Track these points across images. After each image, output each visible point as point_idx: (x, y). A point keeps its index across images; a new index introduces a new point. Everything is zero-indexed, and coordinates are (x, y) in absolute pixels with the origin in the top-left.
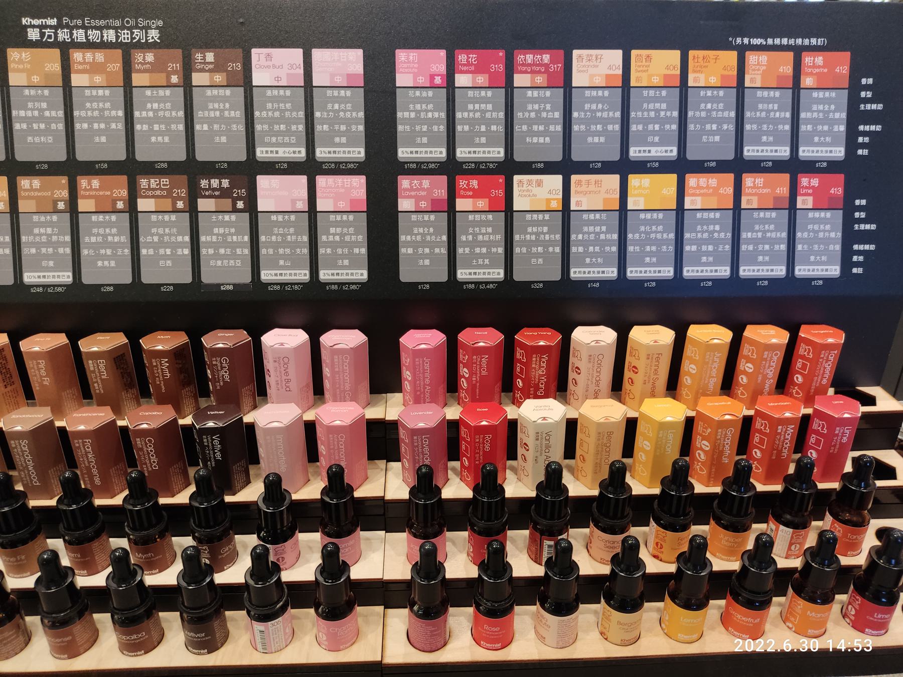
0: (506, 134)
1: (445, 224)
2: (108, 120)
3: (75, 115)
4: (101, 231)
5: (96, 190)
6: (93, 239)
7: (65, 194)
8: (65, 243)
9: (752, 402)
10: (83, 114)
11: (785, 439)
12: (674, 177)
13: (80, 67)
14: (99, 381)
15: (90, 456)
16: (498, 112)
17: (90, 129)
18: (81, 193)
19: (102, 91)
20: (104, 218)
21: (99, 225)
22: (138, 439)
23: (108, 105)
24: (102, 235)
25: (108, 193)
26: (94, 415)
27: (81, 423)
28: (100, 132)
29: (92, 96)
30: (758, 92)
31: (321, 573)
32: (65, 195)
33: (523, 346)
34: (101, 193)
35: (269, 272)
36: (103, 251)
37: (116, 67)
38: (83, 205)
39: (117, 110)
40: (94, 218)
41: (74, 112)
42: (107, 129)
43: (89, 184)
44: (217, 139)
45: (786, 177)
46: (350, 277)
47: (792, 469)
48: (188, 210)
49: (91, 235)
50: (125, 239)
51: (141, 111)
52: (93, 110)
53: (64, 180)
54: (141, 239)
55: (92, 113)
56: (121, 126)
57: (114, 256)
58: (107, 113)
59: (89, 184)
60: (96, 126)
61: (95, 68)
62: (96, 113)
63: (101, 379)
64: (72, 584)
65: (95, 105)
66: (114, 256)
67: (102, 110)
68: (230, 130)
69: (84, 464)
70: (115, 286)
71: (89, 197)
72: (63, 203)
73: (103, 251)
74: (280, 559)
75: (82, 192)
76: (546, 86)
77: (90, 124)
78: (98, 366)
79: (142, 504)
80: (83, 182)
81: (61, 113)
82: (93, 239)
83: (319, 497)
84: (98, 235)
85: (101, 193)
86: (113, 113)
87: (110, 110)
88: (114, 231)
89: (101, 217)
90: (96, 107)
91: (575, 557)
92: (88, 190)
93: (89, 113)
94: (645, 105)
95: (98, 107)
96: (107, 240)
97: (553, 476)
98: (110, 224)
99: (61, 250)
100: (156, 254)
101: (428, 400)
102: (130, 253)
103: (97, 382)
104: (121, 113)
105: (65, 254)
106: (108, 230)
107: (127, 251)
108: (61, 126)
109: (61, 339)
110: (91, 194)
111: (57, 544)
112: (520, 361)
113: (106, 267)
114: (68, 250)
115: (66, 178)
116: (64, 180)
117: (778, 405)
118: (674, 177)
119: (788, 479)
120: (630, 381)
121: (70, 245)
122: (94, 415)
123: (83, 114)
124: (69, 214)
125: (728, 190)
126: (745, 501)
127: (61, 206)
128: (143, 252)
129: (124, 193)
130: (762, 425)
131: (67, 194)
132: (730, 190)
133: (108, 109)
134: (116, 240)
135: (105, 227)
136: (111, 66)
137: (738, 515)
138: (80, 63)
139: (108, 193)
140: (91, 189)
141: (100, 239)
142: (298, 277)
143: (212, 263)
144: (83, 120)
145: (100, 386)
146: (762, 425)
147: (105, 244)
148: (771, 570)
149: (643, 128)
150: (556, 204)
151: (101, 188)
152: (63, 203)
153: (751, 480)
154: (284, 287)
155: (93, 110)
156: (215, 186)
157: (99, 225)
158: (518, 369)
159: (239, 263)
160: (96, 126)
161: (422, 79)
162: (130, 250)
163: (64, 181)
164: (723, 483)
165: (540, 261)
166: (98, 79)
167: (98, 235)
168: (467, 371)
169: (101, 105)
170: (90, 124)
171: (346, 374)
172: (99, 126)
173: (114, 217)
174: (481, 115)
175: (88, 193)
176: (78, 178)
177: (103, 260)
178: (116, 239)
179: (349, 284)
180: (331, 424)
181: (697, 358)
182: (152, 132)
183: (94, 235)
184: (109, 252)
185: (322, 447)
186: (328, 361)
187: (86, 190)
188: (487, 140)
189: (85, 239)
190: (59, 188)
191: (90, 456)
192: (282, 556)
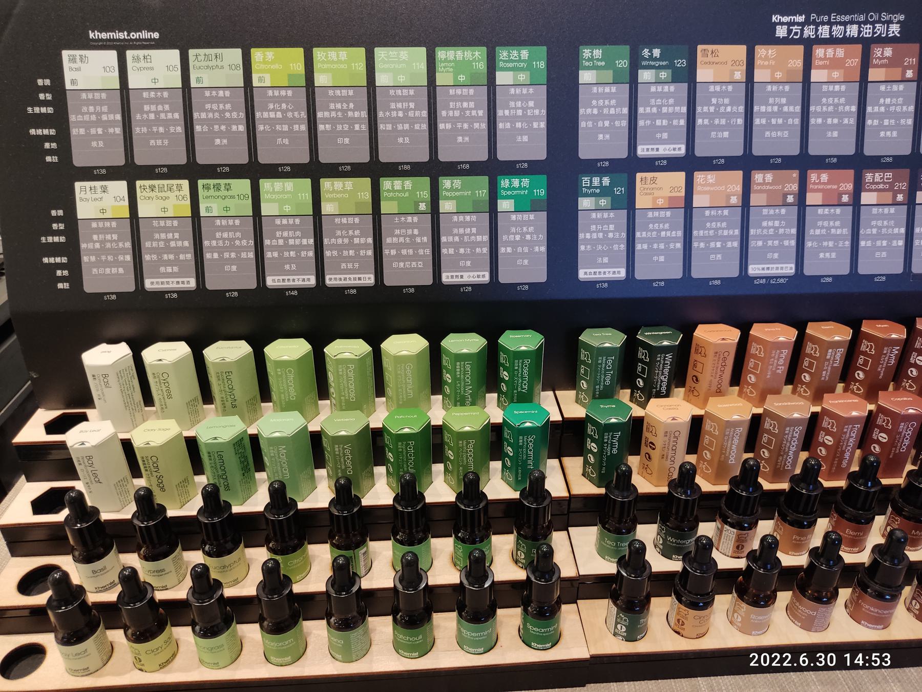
0: (630, 128)
1: (850, 217)
2: (841, 115)
3: (811, 110)
4: (826, 224)
5: (824, 184)
6: (818, 232)
7: (795, 187)
8: (791, 235)
9: (817, 397)
10: (819, 109)
11: (850, 437)
12: (739, 174)
13: (821, 63)
14: (829, 368)
15: (851, 440)
16: (795, 106)
17: (824, 124)
18: (811, 186)
19: (284, 91)
20: (829, 212)
21: (824, 218)
22: (337, 446)
23: (843, 100)
24: (826, 228)
25: (835, 187)
26: (840, 402)
27: (855, 410)
28: (833, 127)
29: (829, 92)
30: (824, 87)
31: (401, 581)
32: (795, 188)
33: (588, 347)
34: (829, 187)
35: (756, 266)
36: (825, 244)
37: (855, 62)
38: (812, 198)
39: (851, 105)
40: (820, 211)
41: (811, 107)
42: (840, 124)
43: (819, 178)
44: (340, 141)
45: (851, 173)
46: (780, 271)
47: (855, 468)
48: (797, 204)
49: (816, 227)
50: (846, 231)
51: (645, 107)
52: (828, 105)
53: (795, 174)
54: (861, 232)
55: (827, 108)
56: (853, 121)
57: (835, 249)
58: (841, 108)
59: (819, 178)
60: (829, 121)
61: (834, 64)
62: (831, 109)
63: (832, 367)
64: (152, 599)
65: (830, 100)
66: (835, 249)
67: (836, 106)
68: (531, 128)
69: (842, 447)
70: (721, 279)
71: (392, 199)
72: (736, 197)
73: (825, 244)
74: (740, 546)
75: (811, 186)
76: (654, 81)
77: (825, 119)
78: (835, 354)
79: (285, 514)
80: (813, 176)
81: (798, 109)
82: (818, 232)
83: (392, 503)
84: (823, 227)
85: (829, 187)
86: (847, 108)
87: (844, 105)
88: (838, 223)
89: (827, 210)
90: (831, 102)
91: (648, 557)
92: (817, 184)
93: (825, 108)
94: (824, 100)
95: (833, 102)
96: (830, 233)
97: (687, 475)
98: (834, 217)
99: (786, 243)
100: (221, 258)
101: (515, 401)
102: (849, 246)
103: (827, 370)
104: (854, 109)
105: (789, 247)
106: (832, 223)
107: (848, 243)
108: (797, 121)
109: (123, 350)
110: (819, 187)
111: (132, 560)
112: (584, 363)
113: (827, 259)
114: (793, 243)
115: (798, 171)
116: (795, 174)
117: (844, 403)
118: (739, 174)
119: (852, 477)
120: (694, 378)
121: (795, 237)
122: (840, 402)
123: (819, 109)
124: (797, 207)
125: (848, 186)
126: (813, 498)
127: (790, 199)
128: (862, 243)
129: (850, 187)
130: (829, 424)
131: (797, 188)
132: (850, 186)
133: (842, 104)
134: (838, 233)
135: (829, 220)
136: (850, 61)
137: (804, 513)
138: (821, 59)
139: (835, 187)
140: (820, 183)
141: (824, 231)
142: (784, 271)
143: (395, 265)
144: (818, 114)
145: (828, 373)
146: (829, 424)
147: (829, 237)
148: (840, 565)
149: (767, 122)
150: (736, 200)
151: (829, 182)
152: (736, 197)
153: (819, 479)
154: (770, 281)
155: (828, 105)
156: (289, 190)
157: (824, 218)
158: (582, 371)
159: (420, 264)
160: (339, 127)
161: (463, 78)
162: (693, 246)
163: (794, 175)
164: (848, 477)
165: (719, 256)
166: (836, 75)
167: (823, 227)
168: (507, 375)
169: (836, 100)
170: (825, 119)
171: (468, 376)
172: (832, 120)
173: (838, 210)
174: (834, 109)
175: (816, 187)
176: (440, 178)
177: (825, 252)
178: (839, 232)
179: (777, 277)
180: (460, 430)
181: (763, 356)
182: (713, 127)
183: (818, 228)
184: (831, 244)
185: (390, 454)
186: (390, 369)
187: (815, 183)
188: (669, 136)
189: (810, 232)
190: (790, 181)
191: (851, 440)
192: (743, 544)
